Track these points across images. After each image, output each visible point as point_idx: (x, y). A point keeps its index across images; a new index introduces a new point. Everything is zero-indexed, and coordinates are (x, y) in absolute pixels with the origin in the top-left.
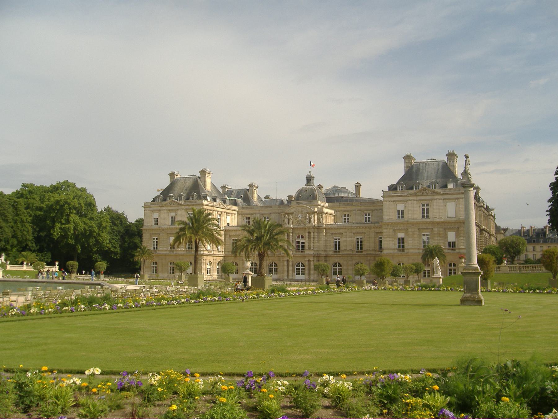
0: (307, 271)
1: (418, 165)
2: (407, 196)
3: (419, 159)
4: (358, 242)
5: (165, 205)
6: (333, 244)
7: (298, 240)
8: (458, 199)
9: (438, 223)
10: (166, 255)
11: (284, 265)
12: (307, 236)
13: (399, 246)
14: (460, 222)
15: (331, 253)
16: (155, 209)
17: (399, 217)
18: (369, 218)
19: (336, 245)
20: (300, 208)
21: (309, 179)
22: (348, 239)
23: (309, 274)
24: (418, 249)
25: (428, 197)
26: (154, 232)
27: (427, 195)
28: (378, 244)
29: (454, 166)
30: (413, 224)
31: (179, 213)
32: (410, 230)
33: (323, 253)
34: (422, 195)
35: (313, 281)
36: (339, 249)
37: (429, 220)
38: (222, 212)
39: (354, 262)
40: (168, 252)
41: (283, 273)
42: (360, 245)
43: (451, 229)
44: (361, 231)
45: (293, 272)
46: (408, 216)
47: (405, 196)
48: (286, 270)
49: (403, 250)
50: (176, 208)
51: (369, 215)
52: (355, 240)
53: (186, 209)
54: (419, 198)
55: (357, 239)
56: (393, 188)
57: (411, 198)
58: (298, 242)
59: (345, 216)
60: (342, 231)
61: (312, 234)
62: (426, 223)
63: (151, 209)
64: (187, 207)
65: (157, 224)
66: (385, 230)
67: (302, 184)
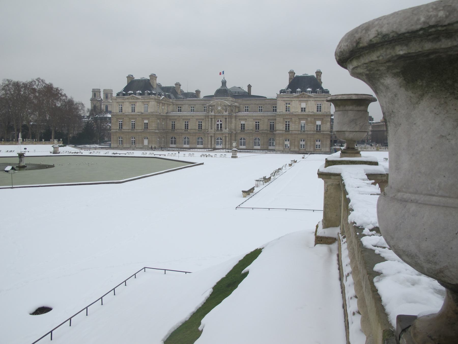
0: (224, 143)
1: (298, 77)
2: (292, 98)
3: (299, 73)
4: (256, 125)
5: (128, 99)
6: (240, 126)
7: (218, 123)
8: (323, 101)
9: (311, 115)
10: (128, 132)
11: (208, 139)
12: (224, 121)
13: (286, 129)
14: (324, 115)
15: (239, 131)
16: (120, 101)
17: (286, 111)
18: (262, 109)
19: (242, 127)
20: (219, 103)
21: (224, 83)
22: (250, 123)
23: (225, 144)
24: (298, 131)
25: (305, 99)
26: (119, 117)
27: (305, 97)
28: (269, 127)
29: (320, 80)
30: (295, 115)
31: (138, 104)
32: (293, 119)
33: (234, 131)
34: (302, 97)
35: (228, 149)
36: (244, 129)
37: (305, 113)
38: (165, 104)
39: (254, 138)
40: (130, 131)
41: (207, 144)
42: (257, 127)
43: (319, 119)
44: (258, 118)
45: (215, 143)
46: (292, 110)
47: (291, 98)
48: (210, 143)
49: (289, 131)
50: (136, 101)
51: (262, 107)
52: (255, 123)
53: (143, 102)
54: (300, 99)
55: (256, 122)
56: (282, 91)
57: (294, 99)
58: (218, 125)
59: (246, 107)
60: (246, 117)
61: (228, 119)
62: (304, 115)
63: (117, 101)
64: (143, 100)
65: (122, 111)
66: (278, 119)
67: (219, 86)
